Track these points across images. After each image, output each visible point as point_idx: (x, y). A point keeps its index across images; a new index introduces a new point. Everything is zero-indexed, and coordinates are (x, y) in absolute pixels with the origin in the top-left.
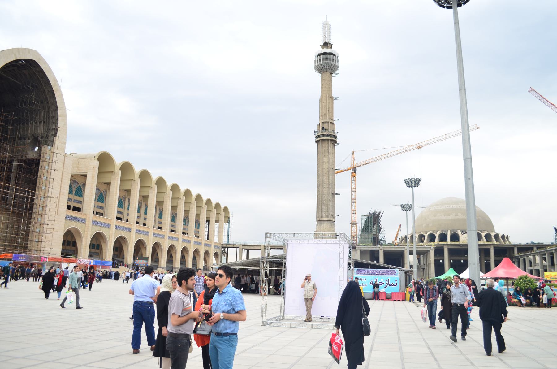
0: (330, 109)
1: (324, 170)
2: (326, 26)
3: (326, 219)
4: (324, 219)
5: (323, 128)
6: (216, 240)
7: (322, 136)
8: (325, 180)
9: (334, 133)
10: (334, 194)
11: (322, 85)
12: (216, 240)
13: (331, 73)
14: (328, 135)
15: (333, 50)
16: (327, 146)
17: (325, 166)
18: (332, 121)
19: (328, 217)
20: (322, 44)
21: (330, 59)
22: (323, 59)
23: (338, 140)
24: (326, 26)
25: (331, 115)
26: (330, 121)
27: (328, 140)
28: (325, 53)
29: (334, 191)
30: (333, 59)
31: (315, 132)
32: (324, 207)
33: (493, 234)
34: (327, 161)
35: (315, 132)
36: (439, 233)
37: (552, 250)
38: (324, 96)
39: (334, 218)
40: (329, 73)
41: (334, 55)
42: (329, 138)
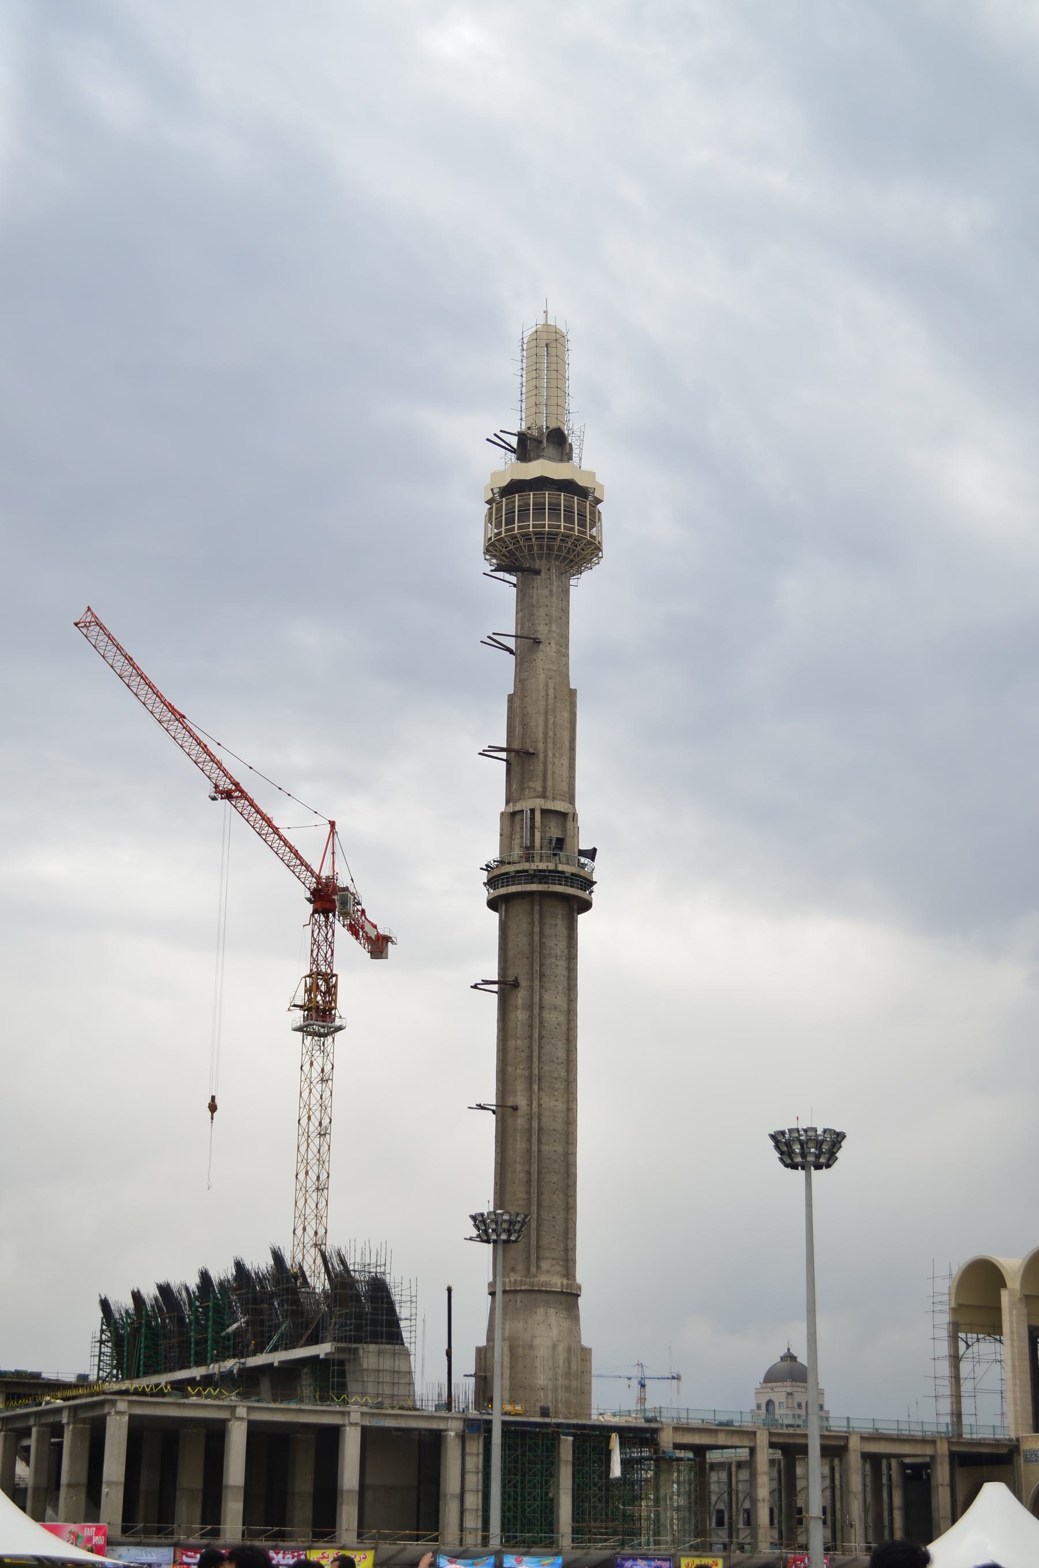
37: (59, 1411)
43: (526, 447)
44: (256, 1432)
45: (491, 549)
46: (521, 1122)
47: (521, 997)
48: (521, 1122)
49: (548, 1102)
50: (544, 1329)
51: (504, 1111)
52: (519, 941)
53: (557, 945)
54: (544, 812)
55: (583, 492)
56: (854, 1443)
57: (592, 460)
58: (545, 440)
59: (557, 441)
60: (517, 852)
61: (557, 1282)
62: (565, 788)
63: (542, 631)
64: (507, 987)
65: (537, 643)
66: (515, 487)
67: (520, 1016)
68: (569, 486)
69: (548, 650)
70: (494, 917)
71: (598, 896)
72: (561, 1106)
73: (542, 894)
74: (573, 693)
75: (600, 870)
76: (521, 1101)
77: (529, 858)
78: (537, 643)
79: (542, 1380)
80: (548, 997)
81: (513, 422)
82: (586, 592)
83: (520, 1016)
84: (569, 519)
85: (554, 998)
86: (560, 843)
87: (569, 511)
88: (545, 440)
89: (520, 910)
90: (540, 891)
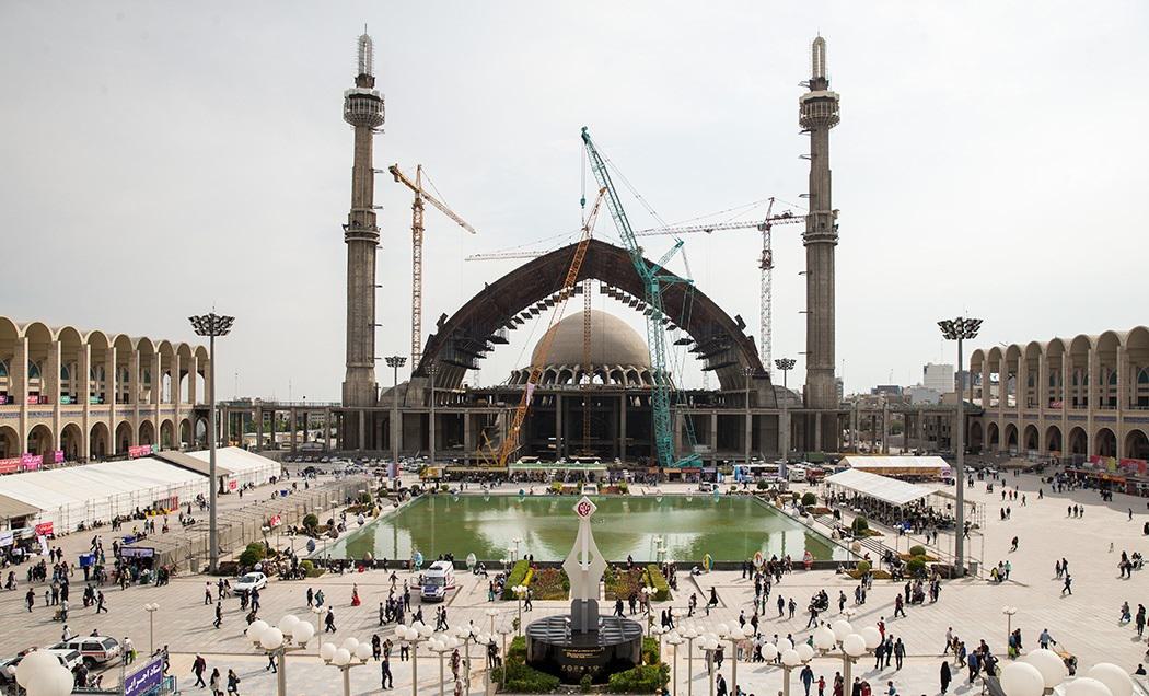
0: (369, 190)
1: (357, 289)
2: (365, 42)
3: (360, 364)
4: (356, 364)
5: (355, 222)
7: (354, 234)
9: (375, 230)
11: (356, 148)
13: (370, 129)
14: (362, 234)
16: (361, 250)
19: (361, 360)
20: (357, 75)
21: (367, 105)
22: (356, 105)
23: (382, 240)
24: (365, 42)
25: (369, 199)
28: (360, 96)
29: (374, 321)
31: (344, 226)
35: (344, 226)
38: (359, 166)
39: (373, 362)
40: (366, 129)
41: (377, 99)
44: (719, 416)
45: (802, 122)
46: (813, 317)
47: (812, 277)
48: (813, 317)
49: (822, 310)
50: (822, 381)
51: (809, 313)
52: (812, 259)
53: (824, 259)
54: (819, 215)
55: (832, 100)
57: (834, 88)
61: (825, 366)
62: (827, 205)
63: (818, 152)
64: (809, 273)
67: (813, 283)
68: (825, 98)
69: (820, 158)
70: (805, 248)
71: (839, 242)
72: (826, 310)
75: (840, 232)
79: (820, 395)
80: (821, 276)
81: (809, 76)
82: (834, 134)
84: (824, 111)
85: (824, 276)
87: (829, 108)
88: (819, 82)
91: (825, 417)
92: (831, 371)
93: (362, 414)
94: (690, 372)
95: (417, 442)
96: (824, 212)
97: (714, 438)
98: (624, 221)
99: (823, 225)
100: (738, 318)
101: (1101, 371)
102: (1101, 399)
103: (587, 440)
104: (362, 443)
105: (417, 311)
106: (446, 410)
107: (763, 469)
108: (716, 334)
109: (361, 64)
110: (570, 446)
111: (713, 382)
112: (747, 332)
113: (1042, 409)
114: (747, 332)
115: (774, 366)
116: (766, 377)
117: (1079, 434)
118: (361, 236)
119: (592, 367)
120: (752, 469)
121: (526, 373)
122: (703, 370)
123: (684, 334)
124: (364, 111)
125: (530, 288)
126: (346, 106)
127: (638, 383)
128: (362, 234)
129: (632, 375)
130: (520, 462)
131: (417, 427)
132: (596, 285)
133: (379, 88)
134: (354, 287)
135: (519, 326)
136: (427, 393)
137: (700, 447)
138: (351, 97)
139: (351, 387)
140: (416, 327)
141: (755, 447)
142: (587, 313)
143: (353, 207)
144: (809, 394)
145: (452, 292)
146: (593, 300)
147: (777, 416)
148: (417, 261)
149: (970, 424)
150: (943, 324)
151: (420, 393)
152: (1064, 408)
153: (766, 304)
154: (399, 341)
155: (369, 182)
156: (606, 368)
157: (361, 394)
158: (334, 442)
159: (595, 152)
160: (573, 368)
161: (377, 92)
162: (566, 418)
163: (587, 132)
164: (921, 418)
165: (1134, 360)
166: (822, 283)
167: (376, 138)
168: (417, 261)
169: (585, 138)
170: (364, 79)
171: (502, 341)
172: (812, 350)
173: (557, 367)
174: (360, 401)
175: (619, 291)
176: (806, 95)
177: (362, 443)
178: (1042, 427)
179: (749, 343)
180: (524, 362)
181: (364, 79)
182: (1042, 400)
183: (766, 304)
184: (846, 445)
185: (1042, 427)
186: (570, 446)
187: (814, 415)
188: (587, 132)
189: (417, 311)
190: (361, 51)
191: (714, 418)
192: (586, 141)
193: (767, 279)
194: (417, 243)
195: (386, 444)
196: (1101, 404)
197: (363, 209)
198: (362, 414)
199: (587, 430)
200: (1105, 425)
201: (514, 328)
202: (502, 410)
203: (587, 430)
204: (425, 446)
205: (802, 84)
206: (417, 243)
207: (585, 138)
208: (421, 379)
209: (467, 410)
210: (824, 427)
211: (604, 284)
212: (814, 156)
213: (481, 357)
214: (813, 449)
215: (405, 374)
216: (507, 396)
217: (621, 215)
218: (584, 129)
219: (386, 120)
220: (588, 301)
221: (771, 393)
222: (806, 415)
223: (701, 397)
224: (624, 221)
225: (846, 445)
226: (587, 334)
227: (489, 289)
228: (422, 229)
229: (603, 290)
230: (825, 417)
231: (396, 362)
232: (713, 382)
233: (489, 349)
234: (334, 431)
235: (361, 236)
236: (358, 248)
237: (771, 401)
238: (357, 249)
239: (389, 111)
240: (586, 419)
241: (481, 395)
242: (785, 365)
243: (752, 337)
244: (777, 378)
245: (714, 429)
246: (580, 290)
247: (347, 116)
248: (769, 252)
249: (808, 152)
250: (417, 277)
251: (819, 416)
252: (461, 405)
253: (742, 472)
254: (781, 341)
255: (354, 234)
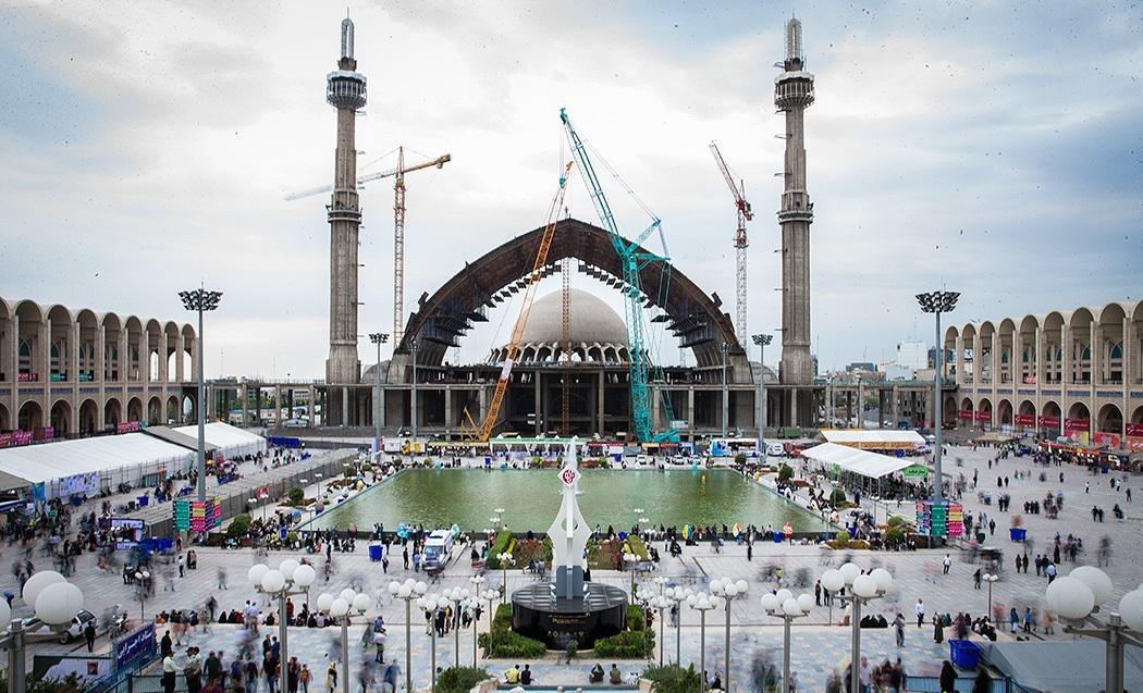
0: (351, 171)
2: (347, 27)
3: (343, 342)
4: (339, 342)
5: (338, 203)
6: (172, 377)
7: (337, 214)
8: (341, 285)
10: (355, 305)
12: (172, 377)
13: (353, 112)
14: (345, 215)
15: (360, 71)
17: (341, 262)
18: (352, 191)
19: (345, 338)
20: (340, 59)
23: (363, 219)
24: (347, 27)
26: (348, 190)
27: (346, 221)
28: (342, 78)
29: (356, 300)
30: (355, 89)
31: (327, 207)
32: (339, 324)
33: (630, 350)
34: (344, 253)
35: (327, 207)
36: (555, 345)
38: (341, 148)
41: (360, 82)
42: (347, 219)
43: (788, 66)
44: (695, 392)
47: (788, 255)
49: (797, 287)
50: (797, 358)
53: (800, 237)
56: (895, 388)
58: (794, 63)
59: (797, 61)
60: (786, 208)
61: (800, 343)
63: (793, 131)
65: (794, 135)
66: (782, 82)
68: (800, 79)
69: (795, 137)
73: (794, 221)
74: (804, 151)
75: (815, 211)
76: (789, 287)
77: (789, 209)
78: (794, 135)
80: (797, 254)
81: (783, 57)
82: (808, 112)
83: (788, 261)
86: (798, 204)
88: (794, 63)
89: (787, 226)
90: (796, 218)
91: (801, 393)
92: (806, 348)
93: (345, 390)
94: (665, 348)
95: (399, 418)
96: (800, 191)
97: (691, 414)
98: (602, 200)
99: (798, 204)
100: (714, 295)
101: (1075, 347)
102: (1074, 374)
103: (566, 417)
104: (345, 420)
105: (399, 290)
106: (427, 386)
107: (740, 444)
108: (693, 313)
109: (344, 47)
110: (549, 422)
111: (690, 359)
112: (723, 309)
113: (1015, 384)
114: (723, 309)
115: (751, 342)
116: (740, 352)
117: (1053, 409)
118: (345, 217)
119: (570, 345)
120: (730, 444)
121: (505, 351)
122: (681, 347)
123: (662, 312)
124: (347, 94)
125: (509, 267)
126: (329, 88)
127: (615, 360)
128: (345, 215)
129: (610, 353)
130: (500, 437)
131: (398, 401)
132: (572, 264)
133: (361, 71)
134: (337, 266)
135: (498, 304)
136: (409, 370)
137: (678, 422)
138: (334, 79)
139: (334, 365)
140: (399, 305)
141: (732, 423)
142: (566, 296)
143: (336, 187)
144: (785, 370)
145: (432, 273)
146: (573, 278)
147: (754, 392)
148: (399, 241)
149: (945, 399)
150: (921, 298)
151: (402, 371)
152: (1038, 383)
153: (742, 282)
154: (384, 317)
155: (352, 163)
156: (584, 345)
157: (344, 371)
158: (318, 419)
159: (573, 133)
160: (551, 345)
161: (360, 75)
162: (545, 395)
163: (565, 112)
164: (895, 394)
165: (1107, 335)
166: (797, 260)
167: (359, 120)
168: (399, 241)
169: (564, 118)
170: (347, 62)
171: (481, 318)
172: (788, 327)
173: (535, 345)
174: (343, 377)
175: (597, 269)
176: (781, 76)
177: (345, 420)
178: (1016, 403)
179: (725, 321)
180: (504, 340)
181: (347, 62)
182: (1016, 374)
183: (742, 282)
184: (821, 420)
185: (1016, 403)
186: (549, 422)
187: (790, 392)
188: (565, 112)
189: (399, 290)
190: (344, 33)
191: (691, 394)
192: (564, 122)
193: (742, 258)
194: (399, 223)
195: (369, 421)
196: (1074, 379)
197: (345, 190)
198: (345, 390)
199: (566, 406)
200: (1109, 401)
201: (494, 306)
202: (482, 386)
203: (566, 406)
204: (407, 422)
205: (776, 65)
206: (399, 223)
207: (564, 118)
208: (403, 357)
209: (448, 386)
210: (800, 405)
211: (582, 263)
212: (789, 136)
213: (461, 334)
214: (789, 424)
215: (387, 352)
216: (488, 373)
217: (599, 194)
218: (562, 110)
219: (368, 101)
220: (566, 279)
221: (747, 369)
222: (782, 390)
223: (677, 374)
224: (602, 200)
225: (821, 420)
226: (566, 312)
227: (469, 267)
228: (403, 209)
229: (581, 269)
230: (801, 393)
231: (378, 338)
232: (690, 359)
233: (469, 327)
234: (318, 408)
235: (345, 217)
236: (341, 228)
237: (747, 378)
238: (339, 229)
239: (370, 94)
240: (565, 397)
241: (460, 373)
242: (762, 340)
243: (727, 315)
244: (754, 353)
245: (691, 404)
246: (559, 269)
247: (330, 99)
248: (744, 230)
249: (783, 132)
250: (399, 256)
251: (794, 392)
252: (442, 381)
253: (719, 446)
254: (755, 314)
255: (337, 214)
